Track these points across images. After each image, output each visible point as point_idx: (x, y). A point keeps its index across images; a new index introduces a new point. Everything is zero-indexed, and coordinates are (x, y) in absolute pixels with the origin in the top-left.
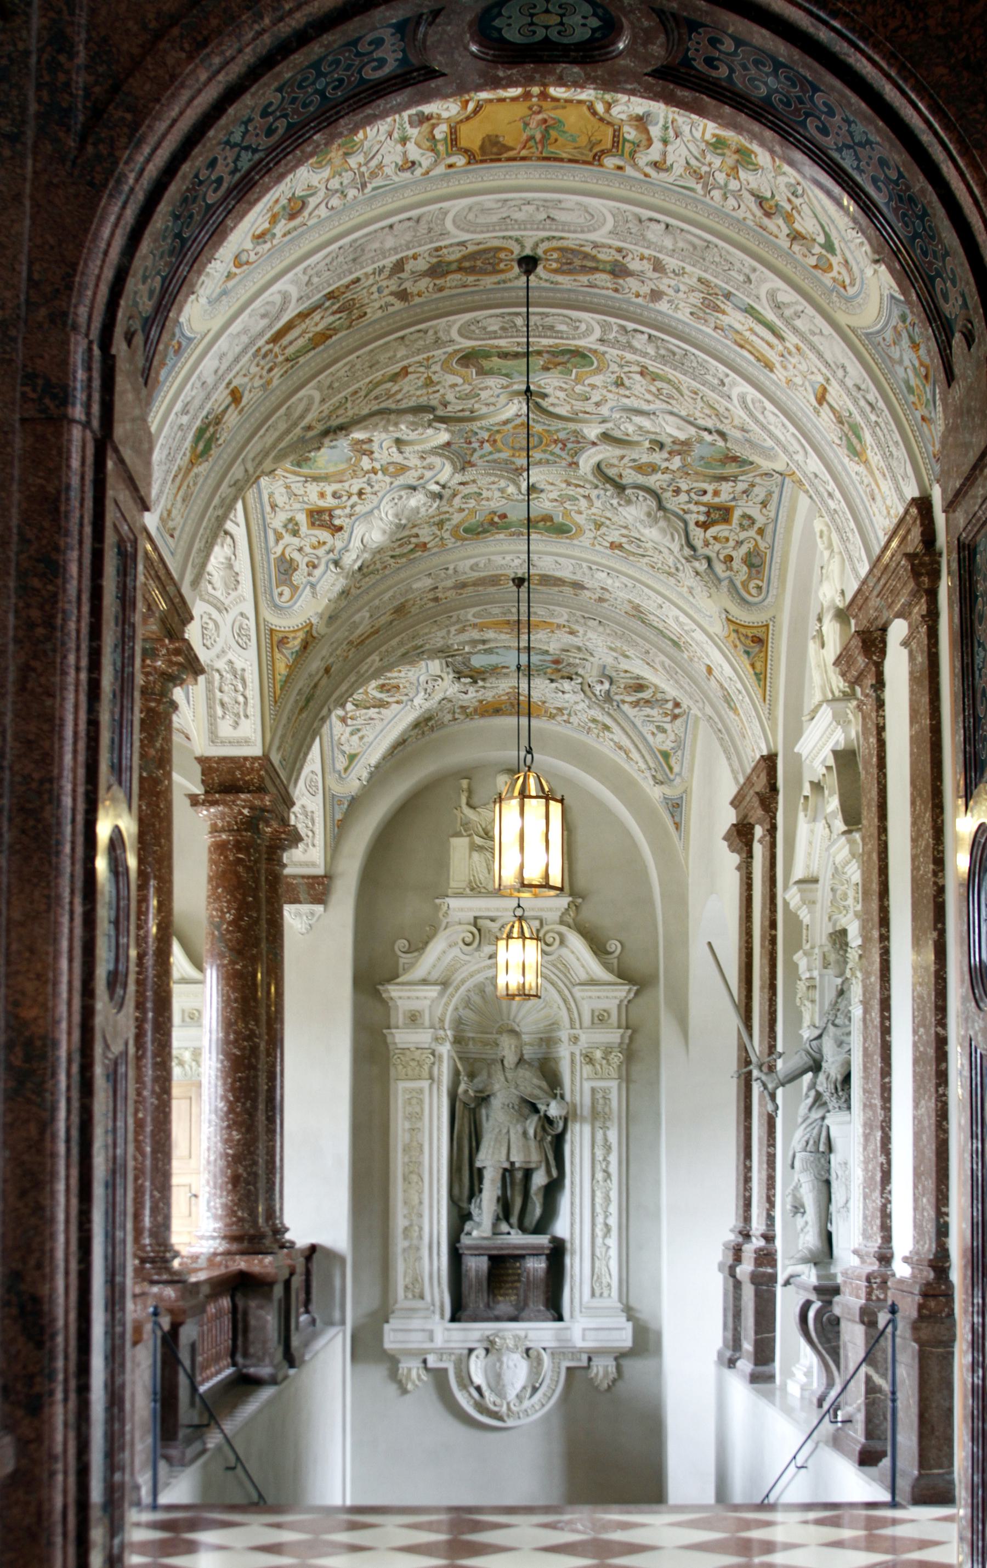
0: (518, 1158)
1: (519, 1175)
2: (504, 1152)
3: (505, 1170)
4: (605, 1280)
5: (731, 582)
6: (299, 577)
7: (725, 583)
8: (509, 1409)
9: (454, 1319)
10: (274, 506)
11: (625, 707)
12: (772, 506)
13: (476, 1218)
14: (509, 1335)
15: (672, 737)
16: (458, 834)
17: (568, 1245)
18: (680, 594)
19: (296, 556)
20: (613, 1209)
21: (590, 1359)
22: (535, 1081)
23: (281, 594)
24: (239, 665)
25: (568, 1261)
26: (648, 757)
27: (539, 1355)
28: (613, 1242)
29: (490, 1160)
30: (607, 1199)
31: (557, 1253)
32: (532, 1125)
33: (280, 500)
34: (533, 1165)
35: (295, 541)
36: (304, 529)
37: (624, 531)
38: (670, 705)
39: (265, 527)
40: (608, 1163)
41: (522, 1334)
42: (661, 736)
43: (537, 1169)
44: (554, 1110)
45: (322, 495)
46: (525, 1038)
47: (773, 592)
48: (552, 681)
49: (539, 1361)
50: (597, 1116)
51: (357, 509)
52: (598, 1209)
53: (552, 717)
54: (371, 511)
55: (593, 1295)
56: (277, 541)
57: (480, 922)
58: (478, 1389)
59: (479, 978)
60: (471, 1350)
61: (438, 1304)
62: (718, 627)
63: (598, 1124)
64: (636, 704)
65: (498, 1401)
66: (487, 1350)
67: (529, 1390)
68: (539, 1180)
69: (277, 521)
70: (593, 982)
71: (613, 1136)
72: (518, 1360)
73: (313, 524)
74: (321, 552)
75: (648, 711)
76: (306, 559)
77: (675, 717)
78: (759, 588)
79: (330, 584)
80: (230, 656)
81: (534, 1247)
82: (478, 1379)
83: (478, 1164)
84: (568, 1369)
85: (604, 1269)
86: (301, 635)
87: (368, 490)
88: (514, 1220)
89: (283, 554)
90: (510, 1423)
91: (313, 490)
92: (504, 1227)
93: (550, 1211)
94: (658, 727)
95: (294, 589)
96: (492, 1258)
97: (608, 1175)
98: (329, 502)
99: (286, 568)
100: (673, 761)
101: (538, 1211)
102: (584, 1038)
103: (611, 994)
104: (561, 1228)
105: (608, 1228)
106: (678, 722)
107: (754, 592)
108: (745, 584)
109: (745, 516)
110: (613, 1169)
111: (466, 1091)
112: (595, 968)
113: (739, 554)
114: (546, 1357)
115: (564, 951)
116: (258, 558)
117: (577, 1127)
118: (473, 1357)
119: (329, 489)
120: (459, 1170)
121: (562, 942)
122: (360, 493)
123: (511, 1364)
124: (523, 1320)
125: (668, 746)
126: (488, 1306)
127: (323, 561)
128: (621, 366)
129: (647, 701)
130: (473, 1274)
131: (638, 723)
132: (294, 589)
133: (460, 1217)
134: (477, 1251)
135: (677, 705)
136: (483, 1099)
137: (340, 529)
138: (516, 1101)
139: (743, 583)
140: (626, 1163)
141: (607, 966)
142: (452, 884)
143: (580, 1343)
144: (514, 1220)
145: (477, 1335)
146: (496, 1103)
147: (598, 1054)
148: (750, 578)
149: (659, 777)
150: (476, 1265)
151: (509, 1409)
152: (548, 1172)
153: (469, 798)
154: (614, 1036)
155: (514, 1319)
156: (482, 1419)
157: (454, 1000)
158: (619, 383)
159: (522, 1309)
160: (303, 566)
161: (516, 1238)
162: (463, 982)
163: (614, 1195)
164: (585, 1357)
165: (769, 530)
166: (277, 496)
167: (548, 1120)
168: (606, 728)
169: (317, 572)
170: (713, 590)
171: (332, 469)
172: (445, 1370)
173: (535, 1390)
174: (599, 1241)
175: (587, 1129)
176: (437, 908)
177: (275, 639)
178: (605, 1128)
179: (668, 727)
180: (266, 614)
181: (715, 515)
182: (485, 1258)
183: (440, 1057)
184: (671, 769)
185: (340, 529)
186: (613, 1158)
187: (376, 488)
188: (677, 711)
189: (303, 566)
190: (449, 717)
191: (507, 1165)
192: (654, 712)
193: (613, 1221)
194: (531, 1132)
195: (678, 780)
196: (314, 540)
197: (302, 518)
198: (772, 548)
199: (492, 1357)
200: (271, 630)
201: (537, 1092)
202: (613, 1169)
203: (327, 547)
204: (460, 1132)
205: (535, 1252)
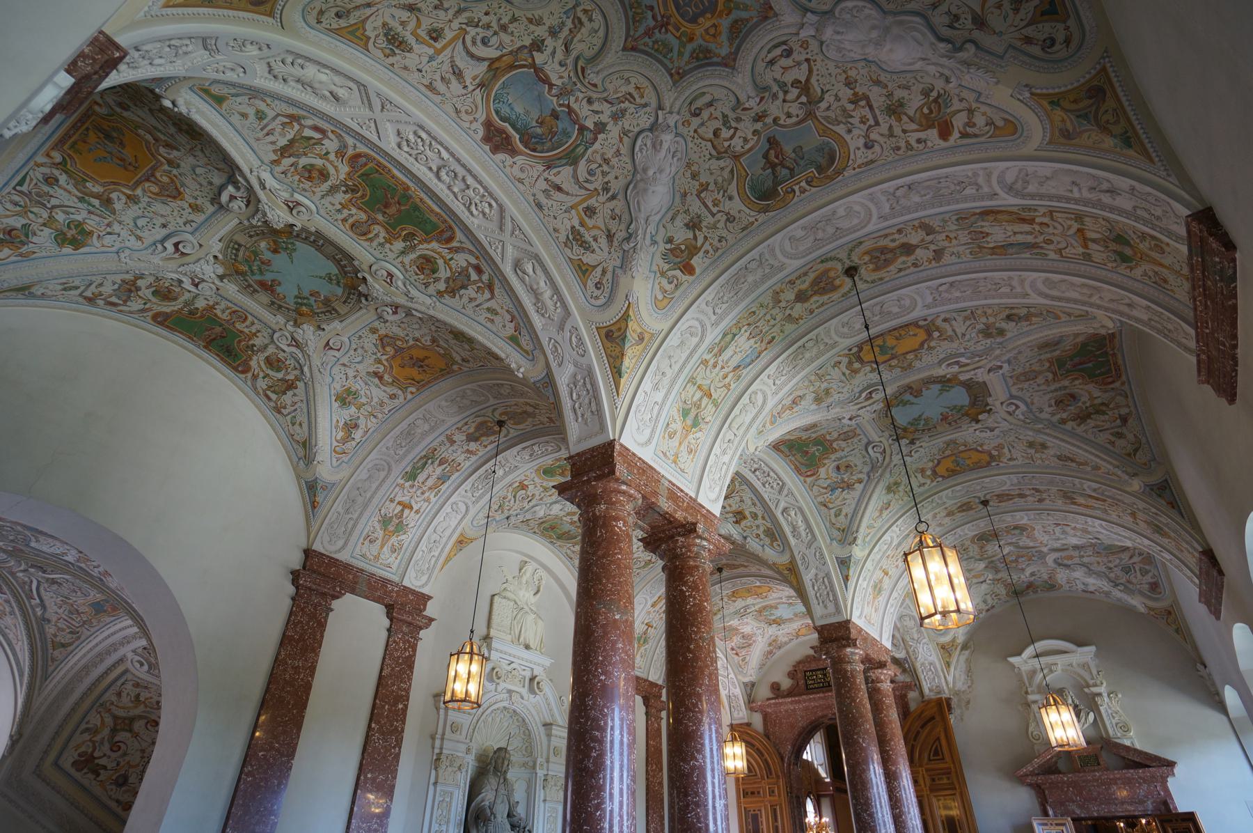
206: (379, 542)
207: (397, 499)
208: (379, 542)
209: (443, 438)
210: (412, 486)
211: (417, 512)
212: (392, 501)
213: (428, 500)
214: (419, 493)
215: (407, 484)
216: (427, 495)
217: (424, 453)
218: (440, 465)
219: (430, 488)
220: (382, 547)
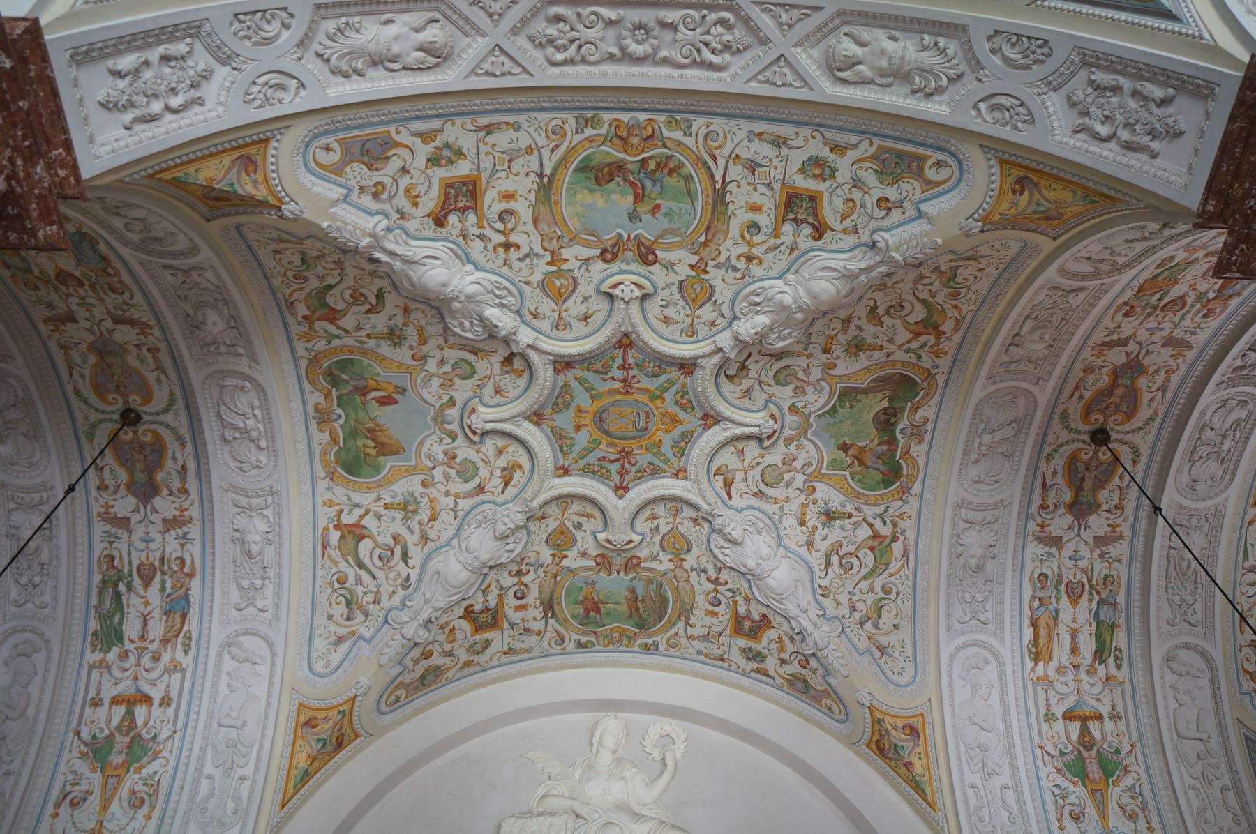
6: (357, 173)
7: (400, 669)
10: (489, 129)
12: (505, 659)
19: (395, 164)
23: (327, 148)
24: (210, 91)
33: (502, 140)
35: (421, 161)
36: (441, 173)
37: (412, 539)
39: (450, 116)
45: (508, 196)
51: (478, 244)
54: (469, 262)
56: (420, 135)
69: (458, 134)
73: (450, 186)
74: (401, 201)
76: (388, 181)
79: (357, 222)
80: (222, 72)
86: (261, 193)
87: (513, 254)
89: (398, 145)
91: (525, 185)
95: (338, 169)
98: (492, 204)
99: (373, 152)
107: (393, 698)
109: (487, 644)
113: (437, 660)
116: (395, 108)
119: (522, 208)
122: (507, 246)
127: (387, 207)
128: (880, 516)
132: (338, 169)
137: (440, 222)
139: (401, 683)
158: (829, 516)
160: (376, 177)
165: (470, 670)
166: (512, 134)
169: (366, 200)
171: (567, 211)
177: (251, 151)
180: (298, 132)
181: (483, 618)
185: (440, 222)
187: (516, 265)
189: (376, 177)
196: (421, 189)
197: (463, 169)
198: (449, 682)
200: (267, 140)
203: (408, 208)
206: (95, 800)
207: (107, 696)
208: (95, 800)
209: (99, 528)
211: (166, 701)
212: (96, 703)
213: (175, 668)
214: (146, 660)
215: (112, 656)
216: (166, 657)
217: (97, 578)
218: (147, 583)
219: (165, 642)
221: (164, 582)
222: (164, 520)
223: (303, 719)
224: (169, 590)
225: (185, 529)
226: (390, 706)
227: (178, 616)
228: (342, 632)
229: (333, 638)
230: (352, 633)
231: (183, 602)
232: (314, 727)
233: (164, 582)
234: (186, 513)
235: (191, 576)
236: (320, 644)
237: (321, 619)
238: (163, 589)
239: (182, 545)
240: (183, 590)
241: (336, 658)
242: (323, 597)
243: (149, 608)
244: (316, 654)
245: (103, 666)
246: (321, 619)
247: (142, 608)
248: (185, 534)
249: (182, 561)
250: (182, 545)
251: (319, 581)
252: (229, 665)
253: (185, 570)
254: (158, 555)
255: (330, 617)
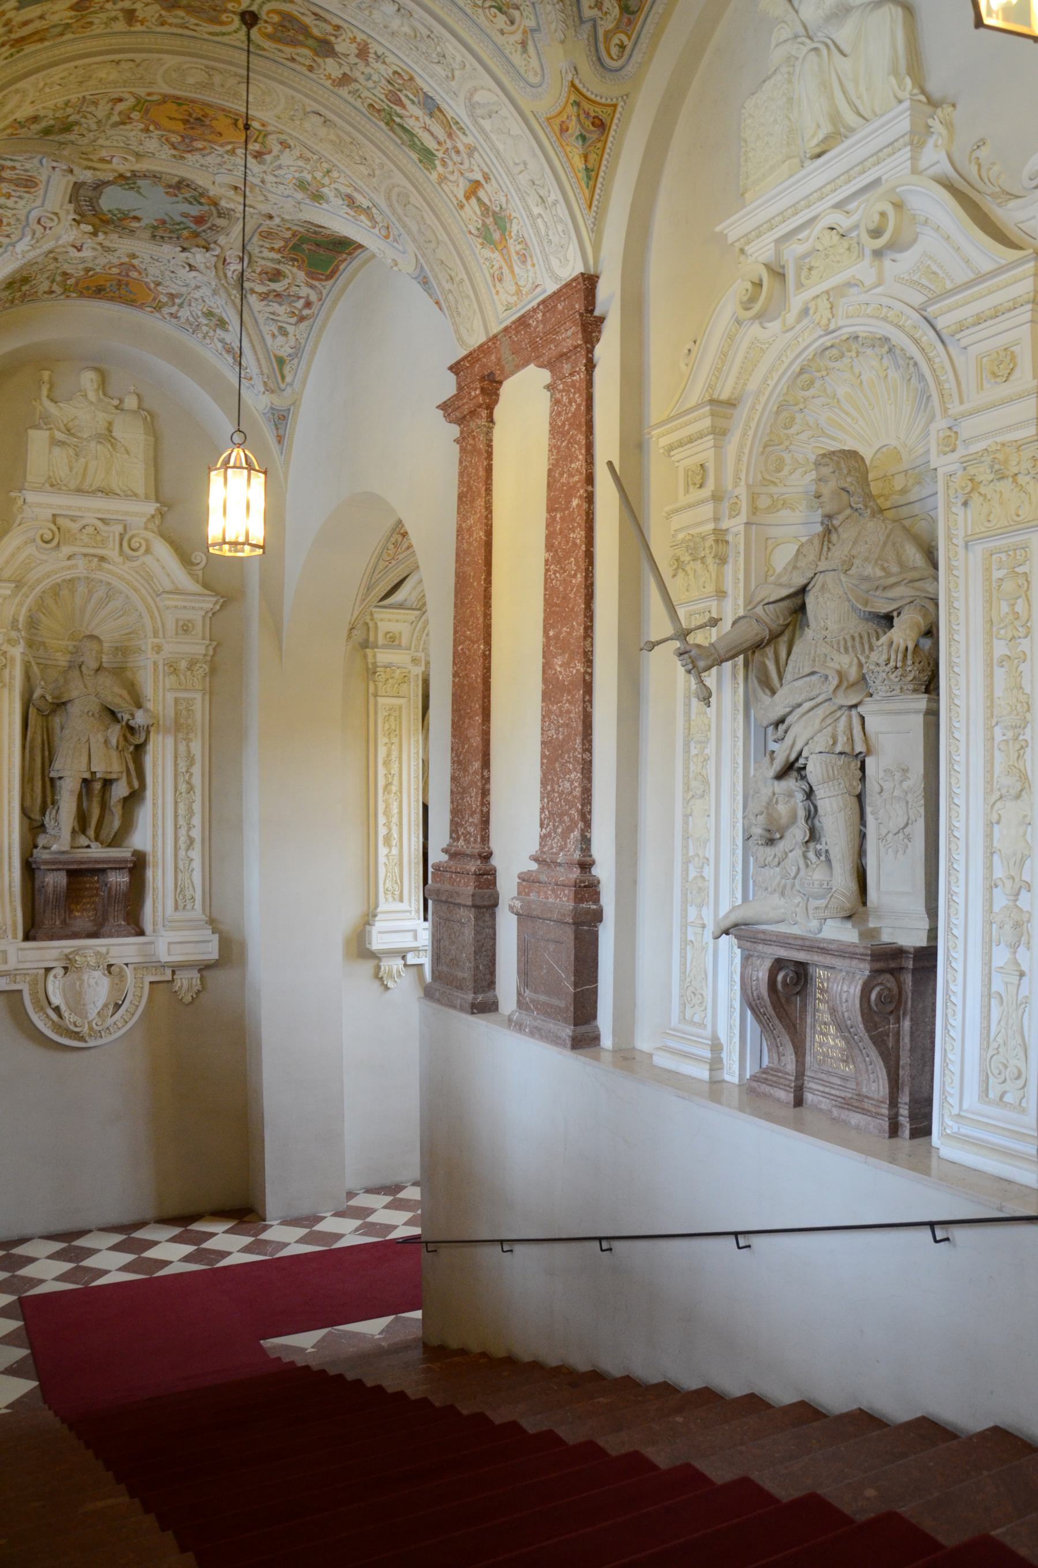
0: (100, 768)
1: (97, 786)
2: (84, 760)
3: (85, 780)
4: (188, 894)
5: (595, 27)
7: (588, 26)
8: (91, 1028)
9: (27, 938)
11: (252, 299)
13: (50, 830)
14: (90, 952)
15: (292, 343)
16: (37, 427)
17: (150, 859)
18: (500, 50)
20: (197, 821)
21: (174, 973)
22: (116, 689)
25: (149, 873)
26: (263, 361)
27: (121, 970)
28: (196, 854)
29: (70, 770)
30: (191, 813)
31: (138, 866)
32: (115, 733)
34: (114, 776)
38: (300, 304)
40: (191, 775)
41: (103, 950)
42: (280, 339)
43: (117, 780)
44: (140, 719)
46: (106, 645)
47: (637, 57)
48: (184, 250)
49: (122, 976)
50: (180, 727)
52: (181, 821)
53: (158, 308)
55: (176, 908)
57: (60, 521)
58: (57, 1010)
59: (57, 578)
60: (48, 970)
61: (9, 922)
62: (551, 99)
63: (180, 736)
64: (264, 297)
65: (79, 1022)
66: (66, 969)
67: (111, 1007)
68: (120, 790)
70: (177, 592)
71: (196, 747)
72: (97, 979)
75: (275, 307)
77: (302, 319)
78: (622, 47)
81: (115, 861)
82: (56, 1000)
83: (53, 774)
84: (151, 983)
85: (187, 882)
88: (91, 832)
90: (91, 1044)
92: (83, 840)
93: (128, 825)
94: (280, 328)
96: (72, 874)
97: (191, 789)
100: (287, 369)
101: (117, 824)
102: (167, 648)
103: (197, 605)
104: (140, 839)
105: (191, 841)
106: (303, 325)
107: (614, 51)
108: (608, 36)
110: (197, 781)
111: (43, 697)
112: (182, 578)
114: (129, 972)
115: (148, 559)
117: (160, 738)
118: (51, 977)
120: (31, 780)
121: (148, 551)
123: (92, 982)
124: (104, 937)
125: (285, 352)
126: (64, 922)
129: (278, 295)
130: (50, 889)
131: (261, 321)
133: (34, 827)
134: (55, 865)
135: (308, 304)
136: (60, 705)
138: (96, 708)
140: (210, 776)
141: (192, 575)
142: (29, 478)
143: (165, 958)
144: (91, 832)
145: (55, 953)
146: (74, 709)
147: (183, 664)
148: (617, 29)
149: (271, 385)
150: (55, 881)
151: (91, 1028)
152: (130, 783)
153: (50, 390)
154: (198, 648)
155: (94, 935)
156: (63, 1041)
157: (29, 600)
159: (102, 925)
161: (97, 852)
162: (39, 581)
163: (197, 807)
164: (169, 972)
167: (131, 729)
168: (222, 324)
170: (571, 32)
172: (20, 991)
173: (117, 1006)
174: (182, 853)
175: (170, 741)
176: (13, 501)
178: (188, 740)
179: (290, 329)
182: (64, 874)
183: (13, 659)
184: (283, 377)
186: (196, 770)
188: (305, 312)
190: (45, 286)
191: (87, 776)
192: (281, 310)
193: (196, 833)
194: (114, 742)
195: (289, 390)
199: (72, 976)
201: (117, 700)
202: (197, 781)
204: (33, 740)
205: (118, 866)
206: (506, 270)
208: (506, 270)
209: (343, 92)
210: (444, 164)
211: (487, 178)
212: (462, 207)
213: (471, 150)
215: (440, 168)
216: (461, 148)
217: (382, 124)
218: (404, 107)
219: (450, 136)
220: (512, 272)
221: (407, 96)
222: (357, 56)
223: (557, 129)
224: (415, 100)
225: (371, 51)
226: (620, 57)
227: (438, 113)
228: (518, 37)
229: (519, 47)
230: (525, 32)
231: (430, 100)
232: (567, 130)
233: (407, 96)
234: (358, 40)
235: (411, 79)
236: (517, 59)
237: (500, 39)
238: (413, 102)
239: (384, 62)
240: (421, 93)
241: (534, 62)
242: (482, 19)
243: (421, 120)
244: (522, 70)
245: (442, 179)
246: (500, 39)
247: (418, 124)
248: (376, 53)
249: (395, 72)
250: (384, 62)
251: (469, 11)
252: (486, 124)
253: (406, 77)
254: (384, 82)
255: (502, 32)
